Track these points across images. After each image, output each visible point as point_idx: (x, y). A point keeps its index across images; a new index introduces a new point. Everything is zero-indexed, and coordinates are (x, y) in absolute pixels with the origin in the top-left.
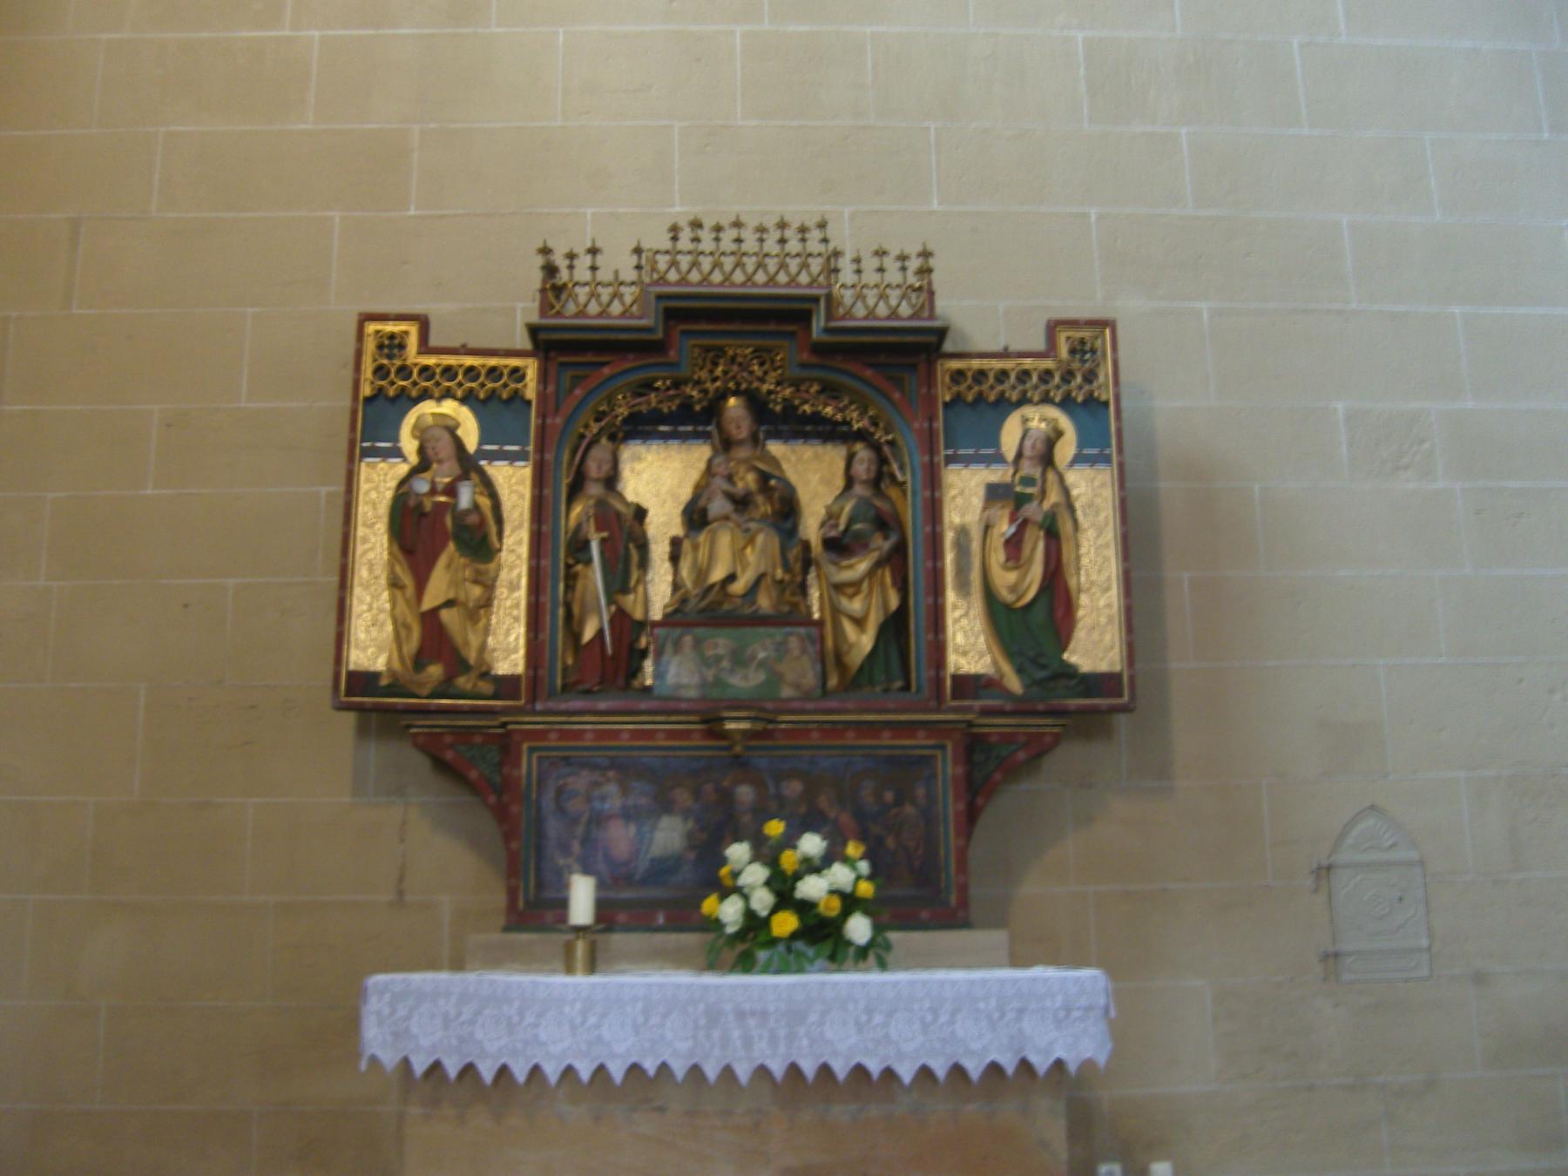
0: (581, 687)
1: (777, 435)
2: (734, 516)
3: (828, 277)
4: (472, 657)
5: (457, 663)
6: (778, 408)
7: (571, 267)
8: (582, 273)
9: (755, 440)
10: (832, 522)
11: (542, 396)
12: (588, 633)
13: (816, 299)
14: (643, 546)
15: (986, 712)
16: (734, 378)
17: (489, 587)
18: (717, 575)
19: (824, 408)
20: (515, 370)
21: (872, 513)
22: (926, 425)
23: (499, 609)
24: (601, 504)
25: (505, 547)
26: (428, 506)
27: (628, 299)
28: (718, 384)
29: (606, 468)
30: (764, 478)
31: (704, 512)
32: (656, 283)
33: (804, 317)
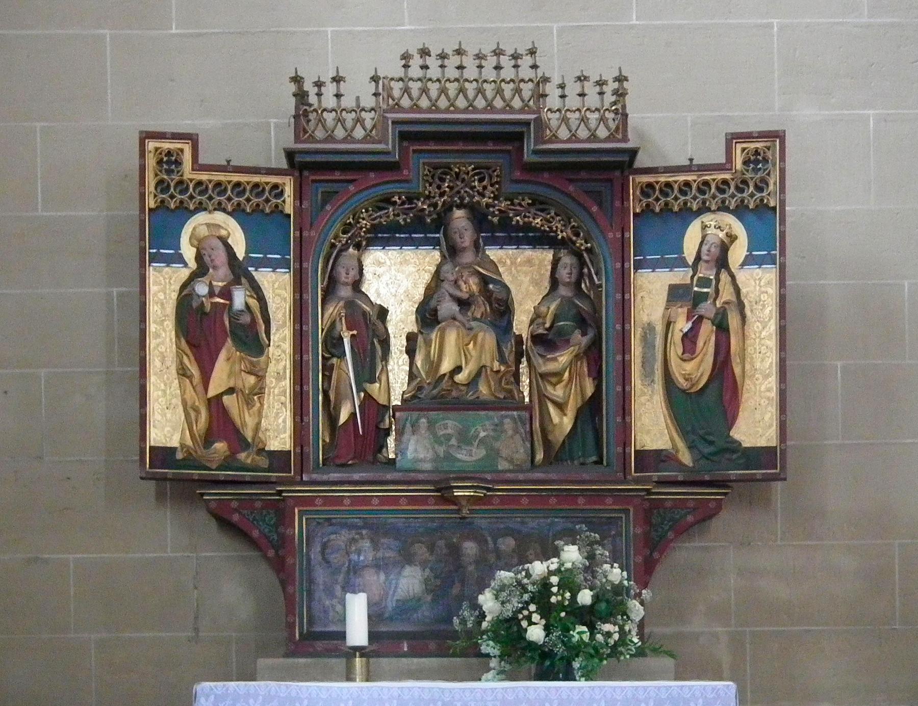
0: (339, 462)
1: (494, 242)
2: (460, 317)
3: (537, 102)
4: (249, 434)
5: (238, 440)
6: (495, 220)
7: (319, 95)
8: (329, 101)
9: (477, 247)
10: (540, 320)
11: (299, 211)
12: (343, 417)
13: (527, 123)
14: (385, 343)
15: (661, 483)
16: (459, 192)
17: (261, 378)
18: (446, 366)
19: (534, 219)
20: (276, 186)
21: (574, 311)
22: (619, 235)
23: (269, 395)
24: (350, 305)
25: (272, 344)
26: (208, 308)
27: (369, 124)
28: (445, 198)
29: (353, 273)
30: (485, 281)
31: (435, 311)
32: (392, 110)
33: (518, 138)
